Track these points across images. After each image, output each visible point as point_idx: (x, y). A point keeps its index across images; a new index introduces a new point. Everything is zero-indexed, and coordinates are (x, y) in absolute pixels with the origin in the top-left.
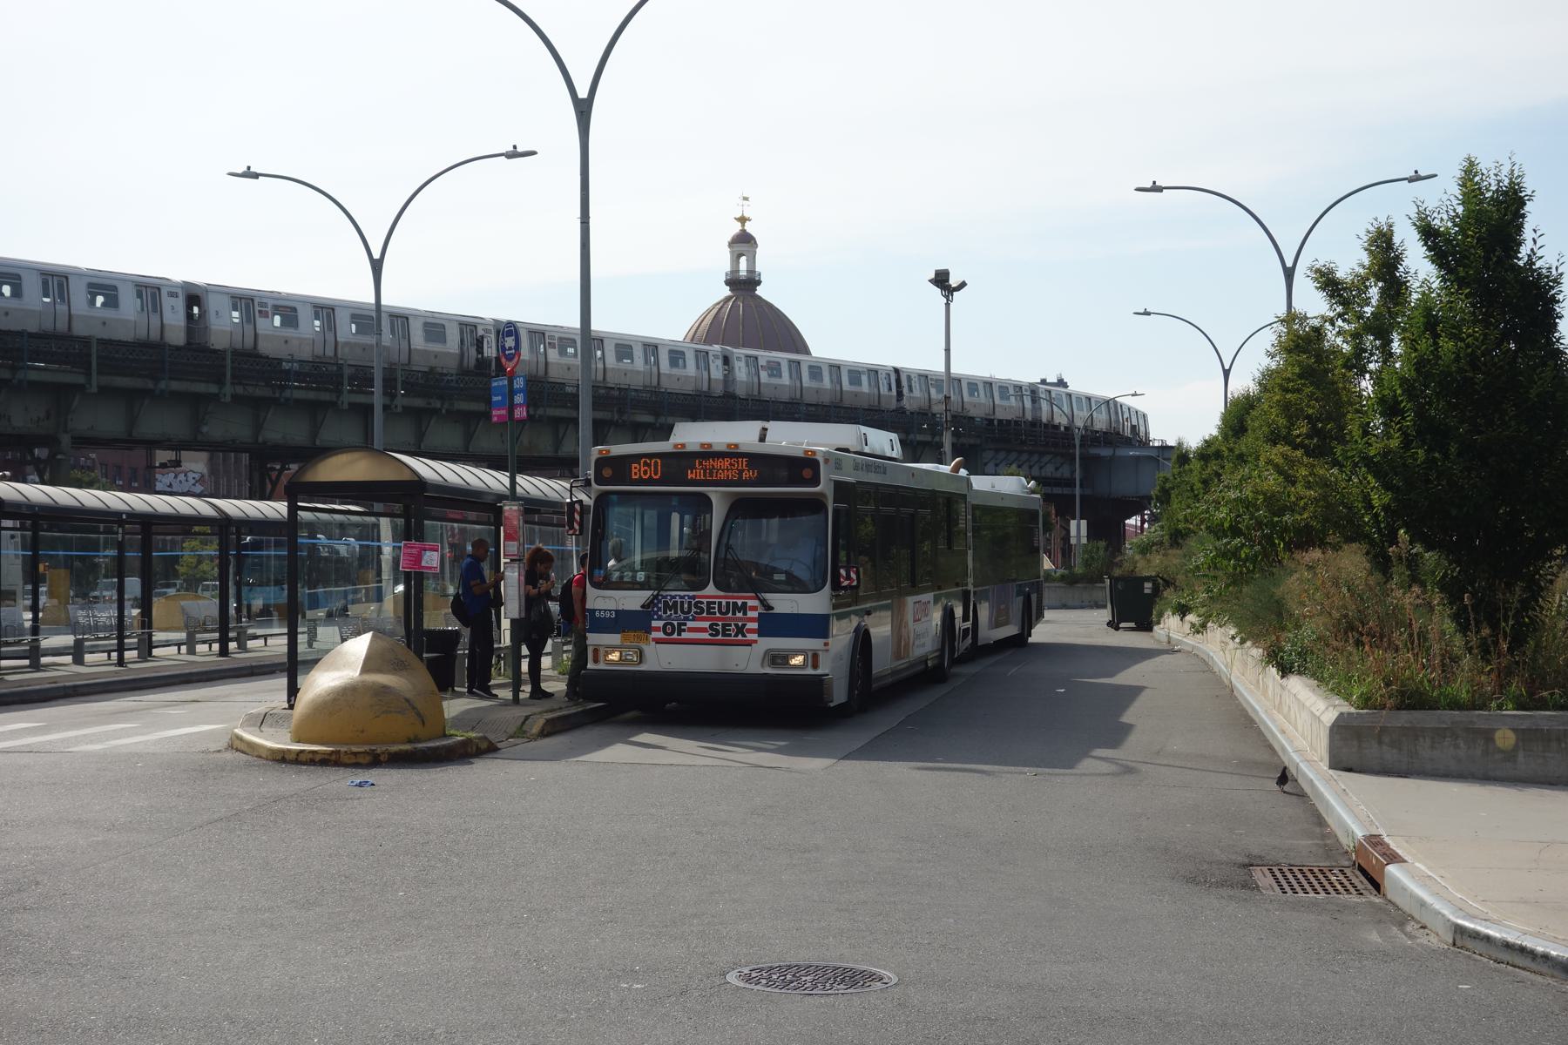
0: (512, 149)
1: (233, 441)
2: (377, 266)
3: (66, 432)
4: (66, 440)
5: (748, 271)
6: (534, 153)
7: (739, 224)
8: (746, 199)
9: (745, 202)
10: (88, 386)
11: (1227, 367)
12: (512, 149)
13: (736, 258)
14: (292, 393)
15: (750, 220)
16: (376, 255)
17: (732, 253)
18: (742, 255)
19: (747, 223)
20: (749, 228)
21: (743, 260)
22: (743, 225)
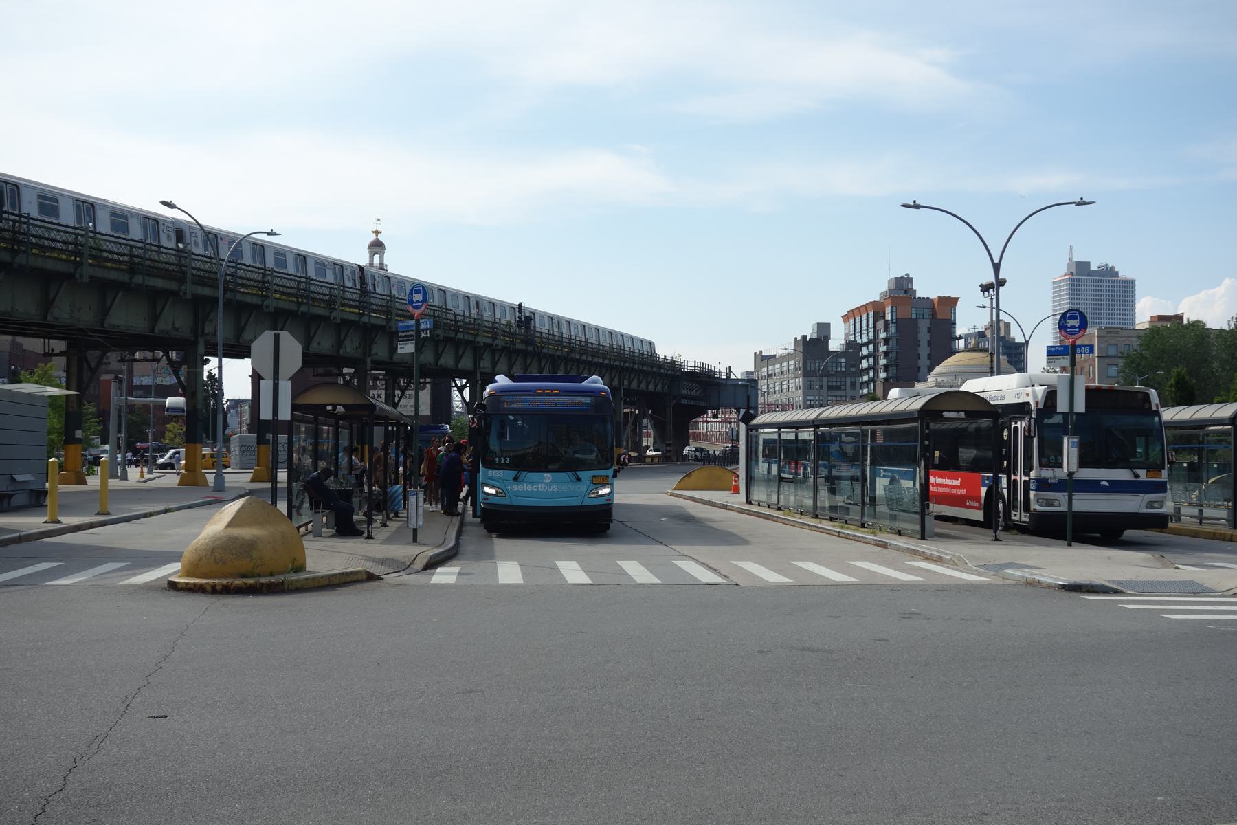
0: (1080, 200)
1: (430, 364)
2: (997, 267)
3: (370, 355)
4: (369, 360)
5: (380, 264)
6: (1094, 203)
7: (374, 235)
8: (378, 220)
9: (378, 222)
10: (387, 327)
11: (1027, 340)
12: (1080, 200)
13: (372, 255)
14: (464, 337)
15: (381, 233)
16: (996, 261)
17: (370, 252)
18: (377, 254)
19: (379, 234)
20: (381, 237)
21: (377, 258)
22: (377, 236)
